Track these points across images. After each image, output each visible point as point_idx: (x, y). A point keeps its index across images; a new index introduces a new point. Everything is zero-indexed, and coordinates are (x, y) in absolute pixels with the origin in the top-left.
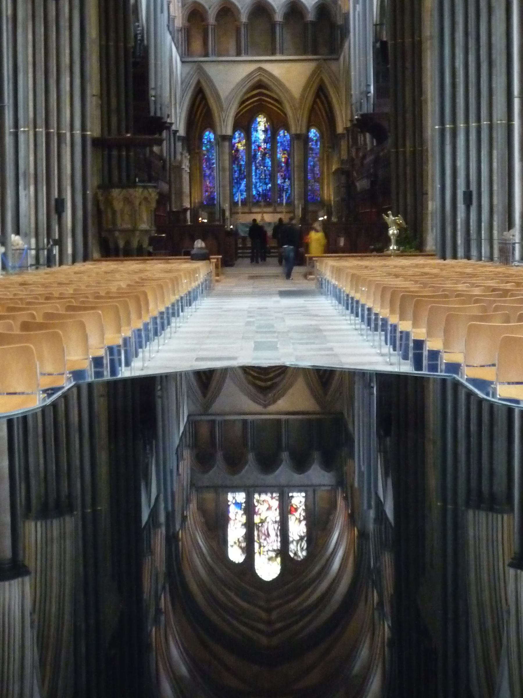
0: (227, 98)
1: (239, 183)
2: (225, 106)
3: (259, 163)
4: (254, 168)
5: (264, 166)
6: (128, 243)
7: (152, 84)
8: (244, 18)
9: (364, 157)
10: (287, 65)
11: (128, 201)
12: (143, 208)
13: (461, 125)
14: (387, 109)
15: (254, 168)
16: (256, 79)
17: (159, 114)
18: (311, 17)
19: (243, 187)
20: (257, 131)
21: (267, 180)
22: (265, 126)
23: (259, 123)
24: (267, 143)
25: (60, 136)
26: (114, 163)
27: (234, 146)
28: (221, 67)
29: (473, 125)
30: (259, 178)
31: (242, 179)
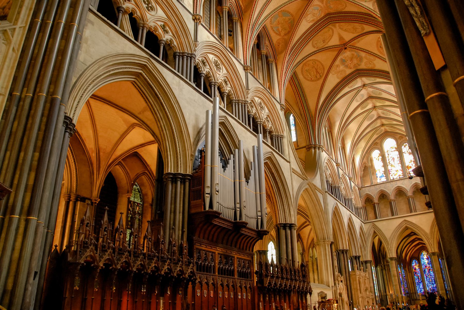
0: (390, 238)
2: (389, 243)
3: (427, 274)
4: (425, 277)
5: (430, 276)
15: (425, 277)
16: (404, 226)
19: (421, 286)
20: (423, 259)
21: (433, 282)
22: (427, 256)
23: (424, 255)
24: (429, 264)
27: (413, 267)
28: (384, 223)
30: (429, 282)
31: (420, 283)
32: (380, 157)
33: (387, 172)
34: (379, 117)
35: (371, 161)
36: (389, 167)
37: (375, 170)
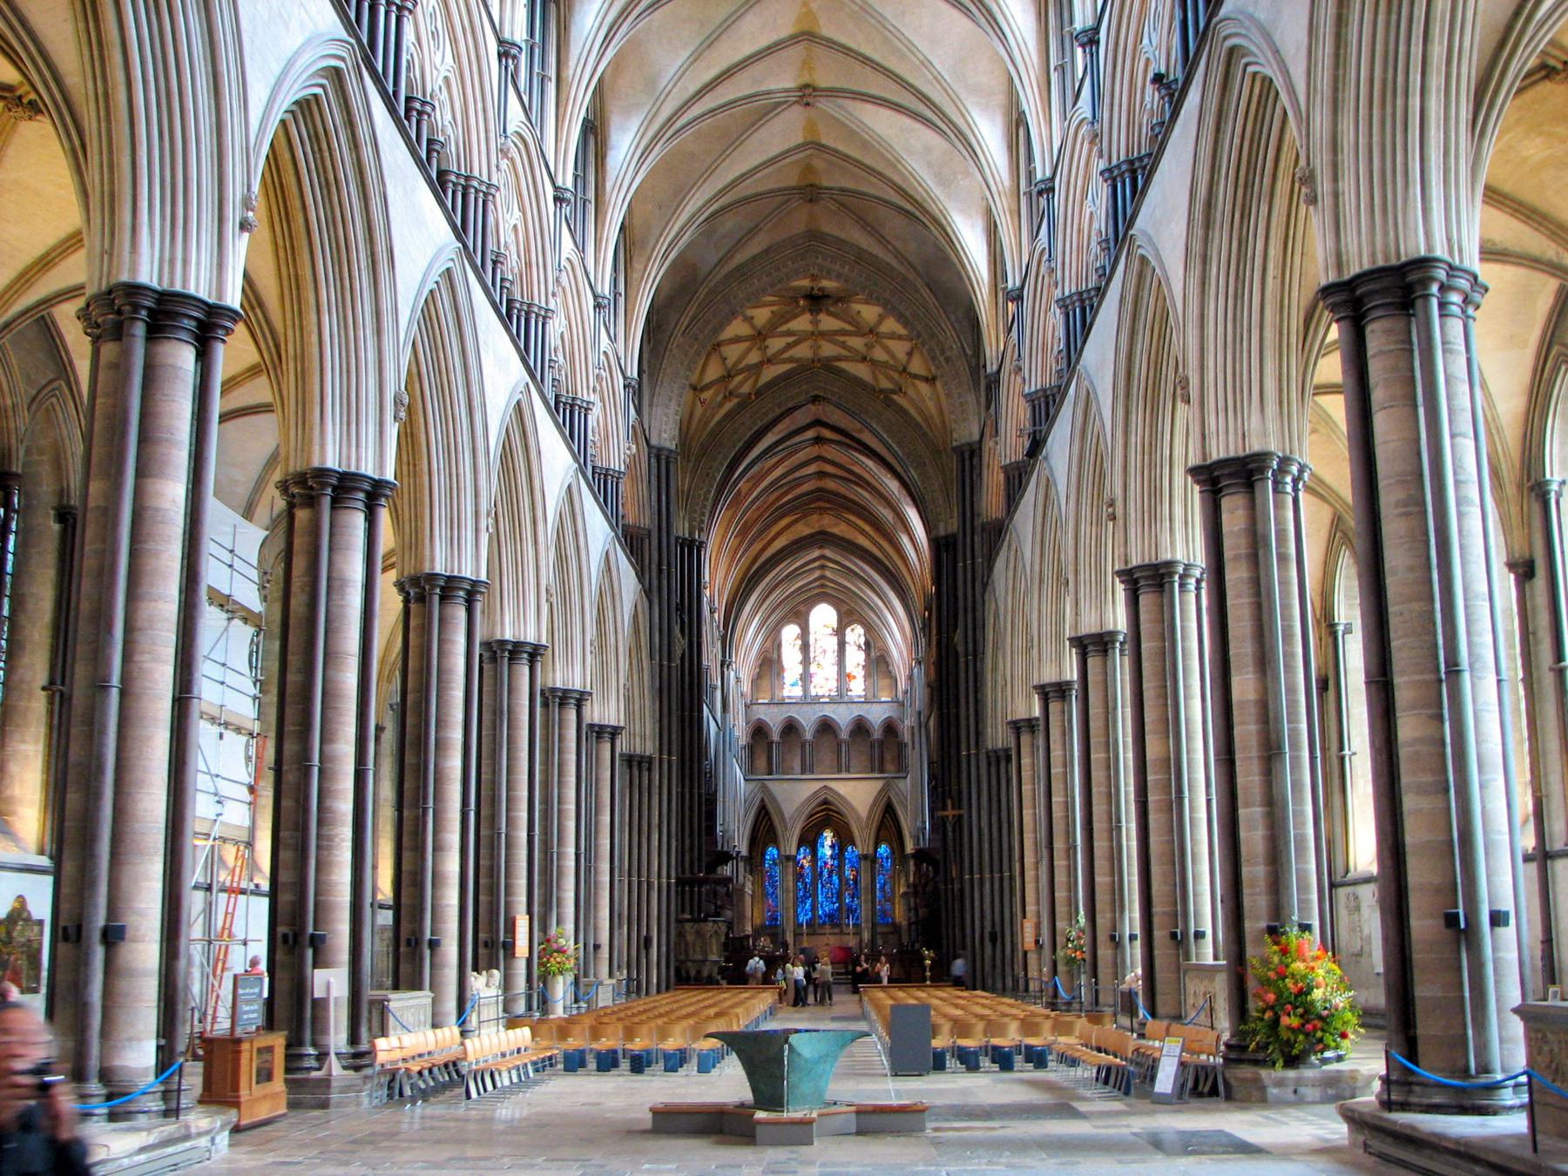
1: (803, 902)
6: (699, 972)
7: (719, 820)
8: (808, 736)
9: (926, 885)
10: (852, 783)
11: (699, 933)
12: (714, 941)
13: (987, 876)
14: (938, 845)
17: (725, 849)
18: (877, 734)
19: (808, 906)
25: (649, 883)
26: (687, 897)
28: (786, 785)
29: (997, 876)
32: (799, 642)
33: (806, 678)
34: (822, 577)
35: (779, 646)
36: (813, 668)
37: (781, 669)
